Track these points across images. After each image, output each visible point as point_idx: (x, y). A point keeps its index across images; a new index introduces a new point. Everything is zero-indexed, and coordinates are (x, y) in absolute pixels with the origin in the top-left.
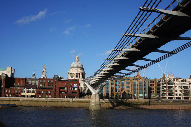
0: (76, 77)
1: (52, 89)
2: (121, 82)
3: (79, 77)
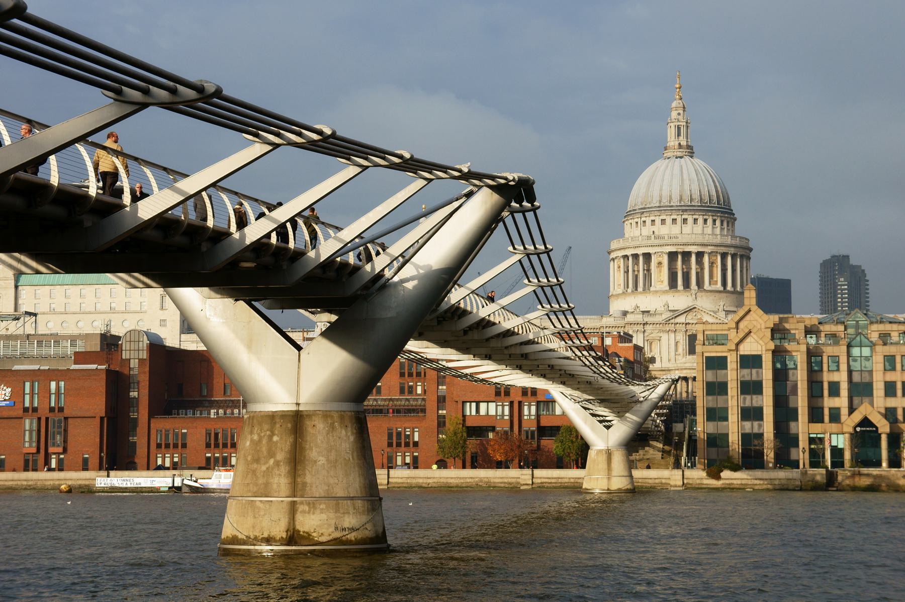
0: (673, 284)
1: (424, 411)
2: (849, 355)
3: (700, 283)
